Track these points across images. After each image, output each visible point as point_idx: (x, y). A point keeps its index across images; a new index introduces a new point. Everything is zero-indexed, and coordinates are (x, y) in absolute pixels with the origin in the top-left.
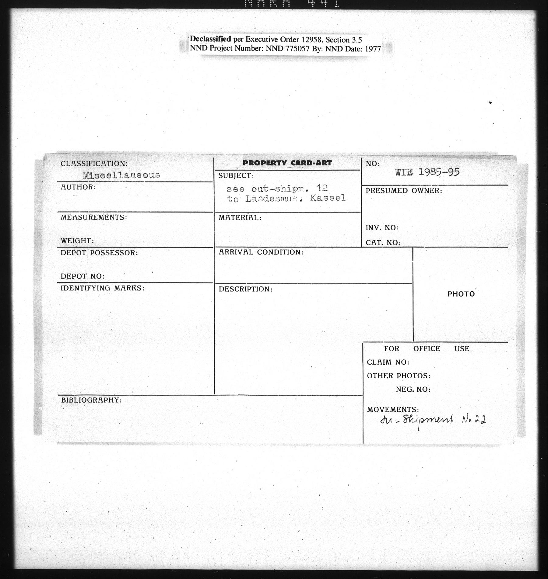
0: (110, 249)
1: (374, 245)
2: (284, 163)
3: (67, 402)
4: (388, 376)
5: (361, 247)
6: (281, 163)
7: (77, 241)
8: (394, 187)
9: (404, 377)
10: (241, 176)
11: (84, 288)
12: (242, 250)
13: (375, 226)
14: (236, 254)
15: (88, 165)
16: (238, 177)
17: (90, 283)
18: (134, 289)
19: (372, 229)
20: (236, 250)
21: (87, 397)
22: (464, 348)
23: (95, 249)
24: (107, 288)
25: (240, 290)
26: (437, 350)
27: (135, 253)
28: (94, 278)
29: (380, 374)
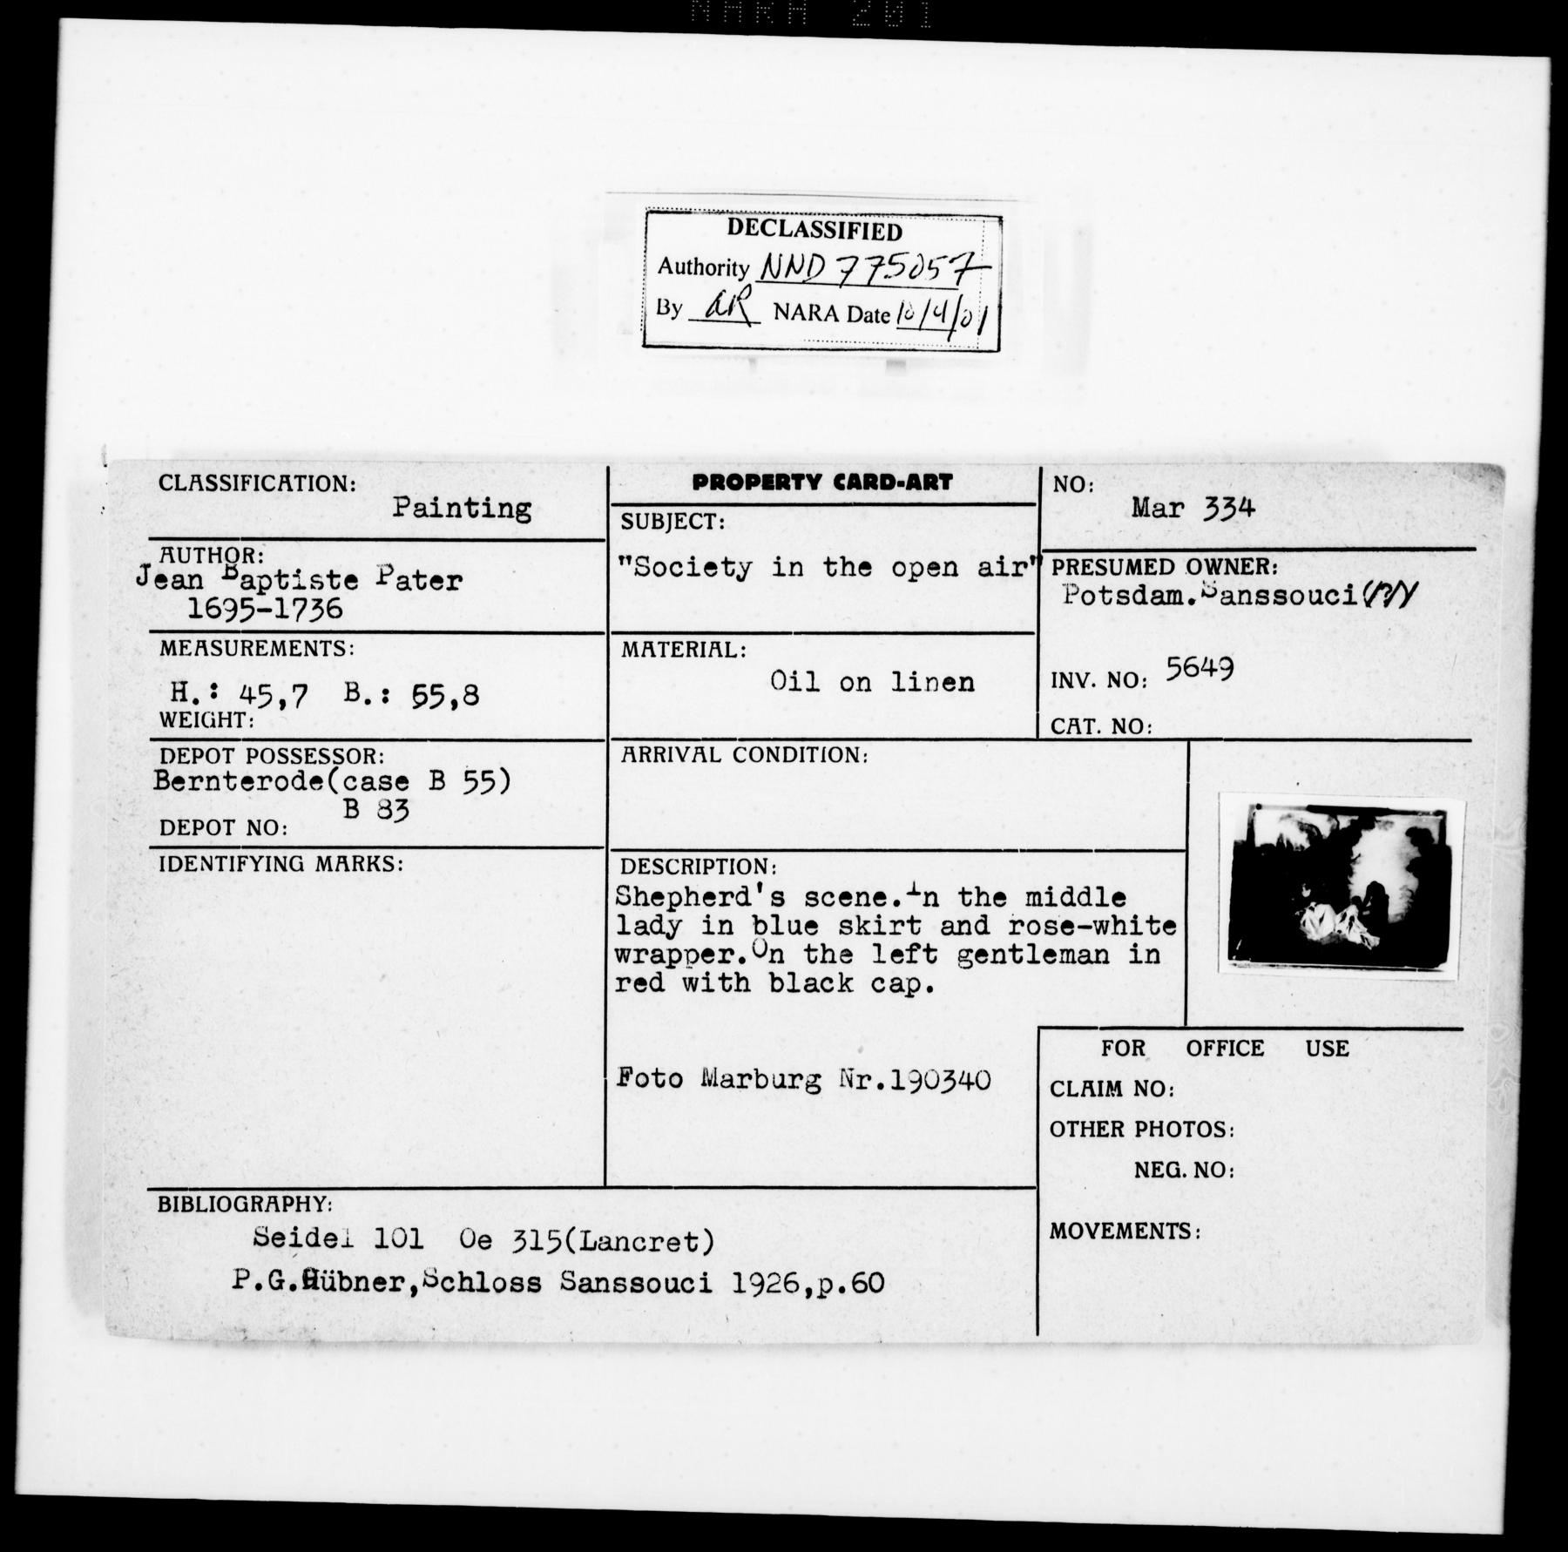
0: (303, 745)
1: (1074, 734)
2: (815, 481)
3: (176, 1210)
4: (1109, 1129)
5: (1038, 739)
6: (805, 483)
7: (208, 722)
8: (1134, 557)
9: (1156, 1132)
10: (686, 521)
11: (227, 863)
12: (688, 748)
13: (1078, 674)
14: (670, 760)
15: (240, 487)
16: (677, 527)
17: (244, 847)
18: (373, 867)
19: (1070, 685)
20: (670, 748)
21: (233, 1195)
22: (1335, 1047)
23: (260, 746)
24: (296, 865)
25: (681, 871)
26: (1254, 1054)
27: (377, 757)
28: (258, 833)
29: (1088, 1125)
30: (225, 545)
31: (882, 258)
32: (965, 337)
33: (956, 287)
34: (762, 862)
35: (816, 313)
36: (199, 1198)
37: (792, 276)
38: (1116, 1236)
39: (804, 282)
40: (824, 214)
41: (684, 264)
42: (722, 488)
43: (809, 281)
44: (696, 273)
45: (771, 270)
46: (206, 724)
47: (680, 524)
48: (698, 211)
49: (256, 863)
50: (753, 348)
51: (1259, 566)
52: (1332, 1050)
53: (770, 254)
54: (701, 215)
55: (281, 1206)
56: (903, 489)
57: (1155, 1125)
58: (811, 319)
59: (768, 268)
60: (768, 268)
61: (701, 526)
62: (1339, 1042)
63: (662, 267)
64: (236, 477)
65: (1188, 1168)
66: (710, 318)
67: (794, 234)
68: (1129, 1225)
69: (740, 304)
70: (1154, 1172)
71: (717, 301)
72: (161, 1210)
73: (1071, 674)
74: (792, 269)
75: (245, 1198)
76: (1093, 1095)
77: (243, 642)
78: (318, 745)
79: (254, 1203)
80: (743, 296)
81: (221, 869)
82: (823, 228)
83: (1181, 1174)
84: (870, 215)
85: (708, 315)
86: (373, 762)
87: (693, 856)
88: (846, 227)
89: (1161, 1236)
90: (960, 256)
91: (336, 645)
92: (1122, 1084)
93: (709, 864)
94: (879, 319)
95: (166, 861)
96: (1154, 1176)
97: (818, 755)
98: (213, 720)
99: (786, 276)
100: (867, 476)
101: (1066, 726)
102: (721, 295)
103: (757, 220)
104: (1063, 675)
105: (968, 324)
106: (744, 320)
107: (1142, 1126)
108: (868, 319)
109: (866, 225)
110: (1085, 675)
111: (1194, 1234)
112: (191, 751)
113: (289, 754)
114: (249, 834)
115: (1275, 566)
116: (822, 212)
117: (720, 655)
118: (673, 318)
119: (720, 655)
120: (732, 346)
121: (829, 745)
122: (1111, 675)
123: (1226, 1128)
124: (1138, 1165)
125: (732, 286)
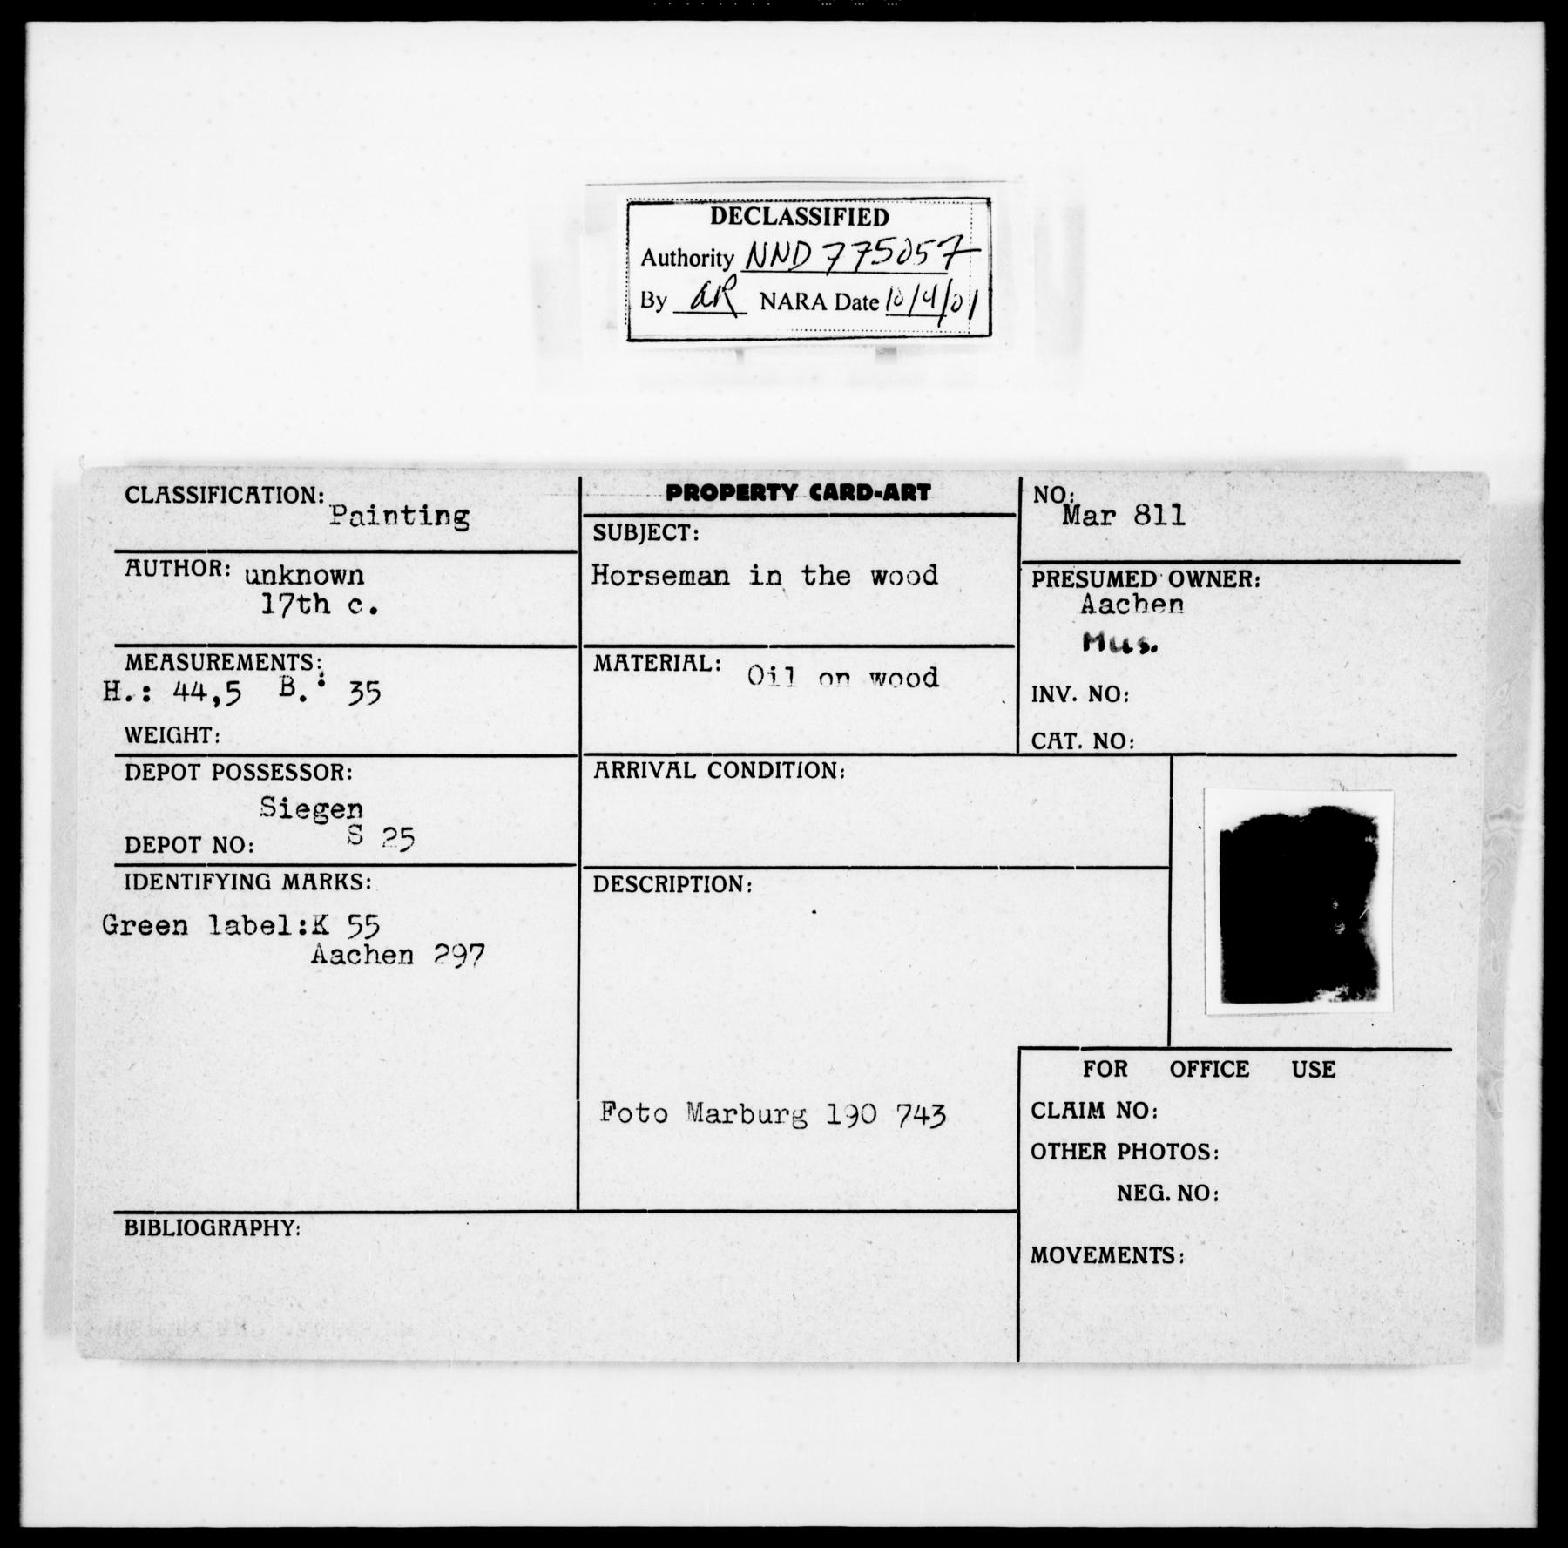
0: (270, 761)
1: (1055, 749)
2: (790, 492)
3: (143, 1234)
4: (1091, 1151)
5: (1018, 754)
6: (781, 493)
7: (174, 737)
8: (1116, 569)
9: (1140, 1154)
10: (660, 532)
11: (192, 881)
12: (661, 763)
13: (1058, 688)
14: (644, 776)
15: (207, 498)
16: (650, 539)
17: (210, 865)
18: (341, 885)
19: (1051, 699)
20: (644, 764)
21: (200, 1219)
22: (1321, 1068)
23: (225, 762)
24: (263, 884)
25: (655, 889)
26: (1239, 1075)
27: (345, 773)
28: (224, 850)
29: (1069, 1147)
30: (191, 558)
31: (869, 244)
32: (955, 322)
33: (945, 271)
34: (738, 880)
35: (803, 302)
36: (165, 1222)
37: (778, 265)
38: (1098, 1260)
39: (790, 271)
40: (808, 201)
41: (667, 255)
42: (696, 499)
43: (795, 270)
44: (679, 265)
45: (756, 260)
46: (172, 739)
47: (654, 536)
48: (679, 201)
49: (222, 881)
50: (739, 340)
51: (1242, 578)
52: (1319, 1072)
53: (755, 243)
54: (683, 205)
55: (249, 1231)
56: (880, 500)
57: (1138, 1147)
58: (798, 308)
59: (753, 257)
60: (753, 257)
61: (675, 537)
62: (1325, 1063)
63: (645, 259)
64: (203, 488)
65: (1171, 1191)
66: (695, 310)
67: (778, 222)
68: (1111, 1249)
69: (725, 294)
70: (1137, 1196)
71: (702, 292)
72: (127, 1233)
73: (1052, 687)
74: (777, 258)
75: (212, 1222)
76: (1074, 1116)
77: (209, 656)
78: (285, 761)
79: (221, 1226)
80: (728, 286)
81: (187, 888)
82: (808, 214)
83: (1165, 1197)
84: (855, 200)
85: (693, 307)
86: (341, 778)
87: (667, 873)
88: (832, 213)
89: (1144, 1261)
90: (949, 239)
91: (303, 659)
92: (1104, 1106)
93: (683, 882)
94: (868, 306)
95: (132, 879)
96: (1137, 1199)
97: (794, 770)
98: (179, 735)
99: (772, 265)
100: (843, 486)
101: (1046, 741)
102: (706, 286)
103: (740, 209)
104: (1043, 689)
105: (958, 309)
106: (730, 311)
107: (1124, 1149)
108: (857, 306)
109: (852, 210)
110: (1066, 689)
111: (1177, 1258)
112: (157, 768)
113: (255, 770)
114: (215, 851)
115: (1258, 579)
116: (807, 199)
117: (695, 669)
118: (658, 311)
119: (695, 669)
120: (718, 338)
121: (806, 760)
122: (1092, 689)
123: (1211, 1150)
124: (1121, 1188)
125: (717, 276)
